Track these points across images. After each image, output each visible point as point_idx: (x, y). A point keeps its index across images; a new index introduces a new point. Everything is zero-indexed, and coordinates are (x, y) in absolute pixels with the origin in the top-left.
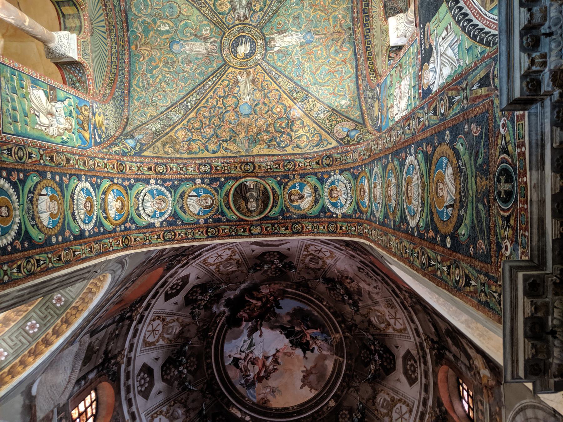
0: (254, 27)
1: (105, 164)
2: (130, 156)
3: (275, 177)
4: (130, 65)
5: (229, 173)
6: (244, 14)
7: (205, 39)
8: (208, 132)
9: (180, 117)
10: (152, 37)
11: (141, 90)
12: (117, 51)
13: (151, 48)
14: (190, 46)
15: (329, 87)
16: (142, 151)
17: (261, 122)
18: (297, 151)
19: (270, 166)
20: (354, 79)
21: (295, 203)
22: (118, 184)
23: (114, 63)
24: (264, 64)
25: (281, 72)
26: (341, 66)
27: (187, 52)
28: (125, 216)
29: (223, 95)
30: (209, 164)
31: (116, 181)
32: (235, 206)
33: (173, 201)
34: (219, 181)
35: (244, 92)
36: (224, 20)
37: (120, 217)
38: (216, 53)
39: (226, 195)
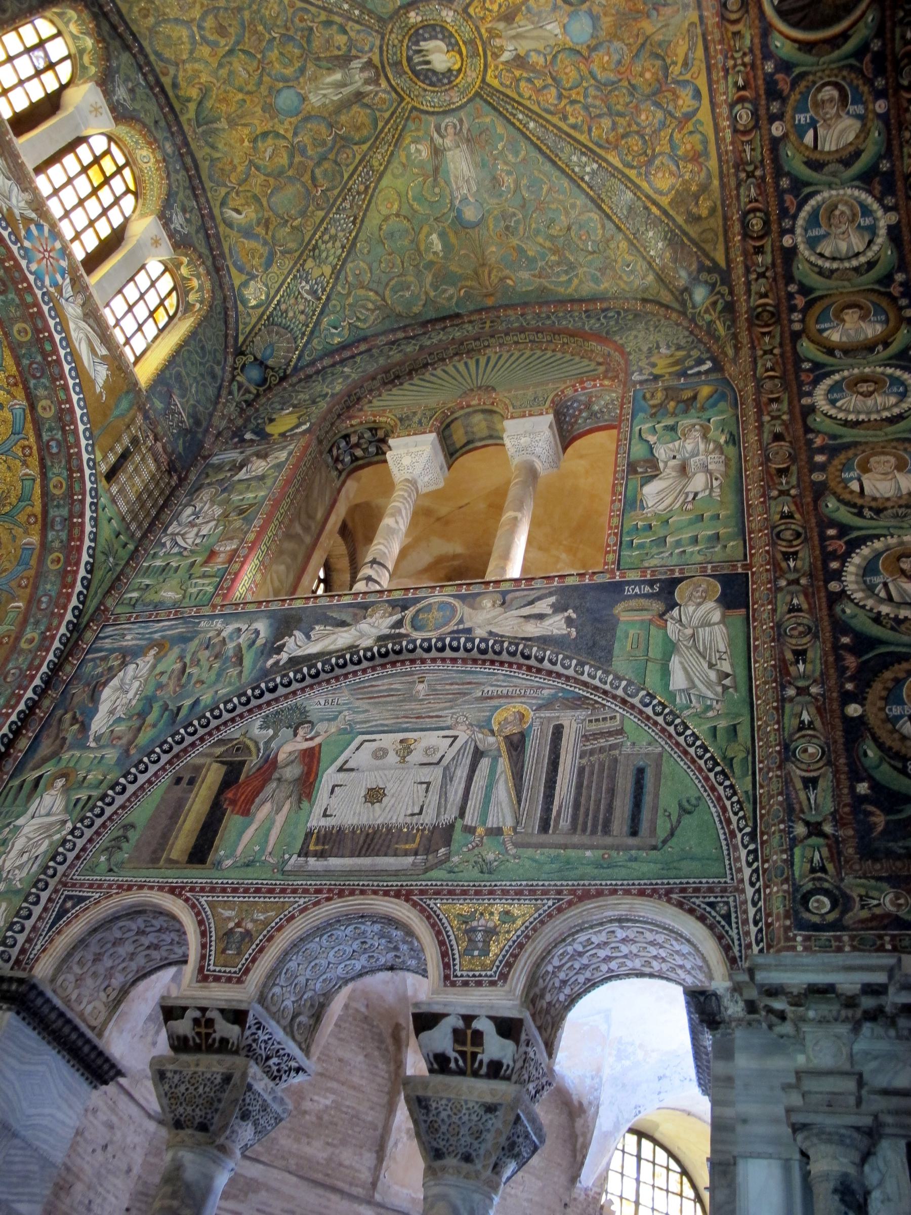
0: (383, 38)
1: (765, 352)
2: (731, 293)
4: (525, 304)
5: (751, 50)
6: (362, 70)
8: (649, 116)
9: (623, 187)
12: (507, 334)
13: (483, 265)
14: (460, 183)
16: (715, 268)
22: (803, 321)
27: (474, 189)
28: (874, 297)
29: (554, 91)
30: (732, 106)
31: (797, 327)
33: (830, 186)
34: (772, 75)
35: (538, 38)
36: (387, 115)
37: (879, 310)
38: (461, 121)
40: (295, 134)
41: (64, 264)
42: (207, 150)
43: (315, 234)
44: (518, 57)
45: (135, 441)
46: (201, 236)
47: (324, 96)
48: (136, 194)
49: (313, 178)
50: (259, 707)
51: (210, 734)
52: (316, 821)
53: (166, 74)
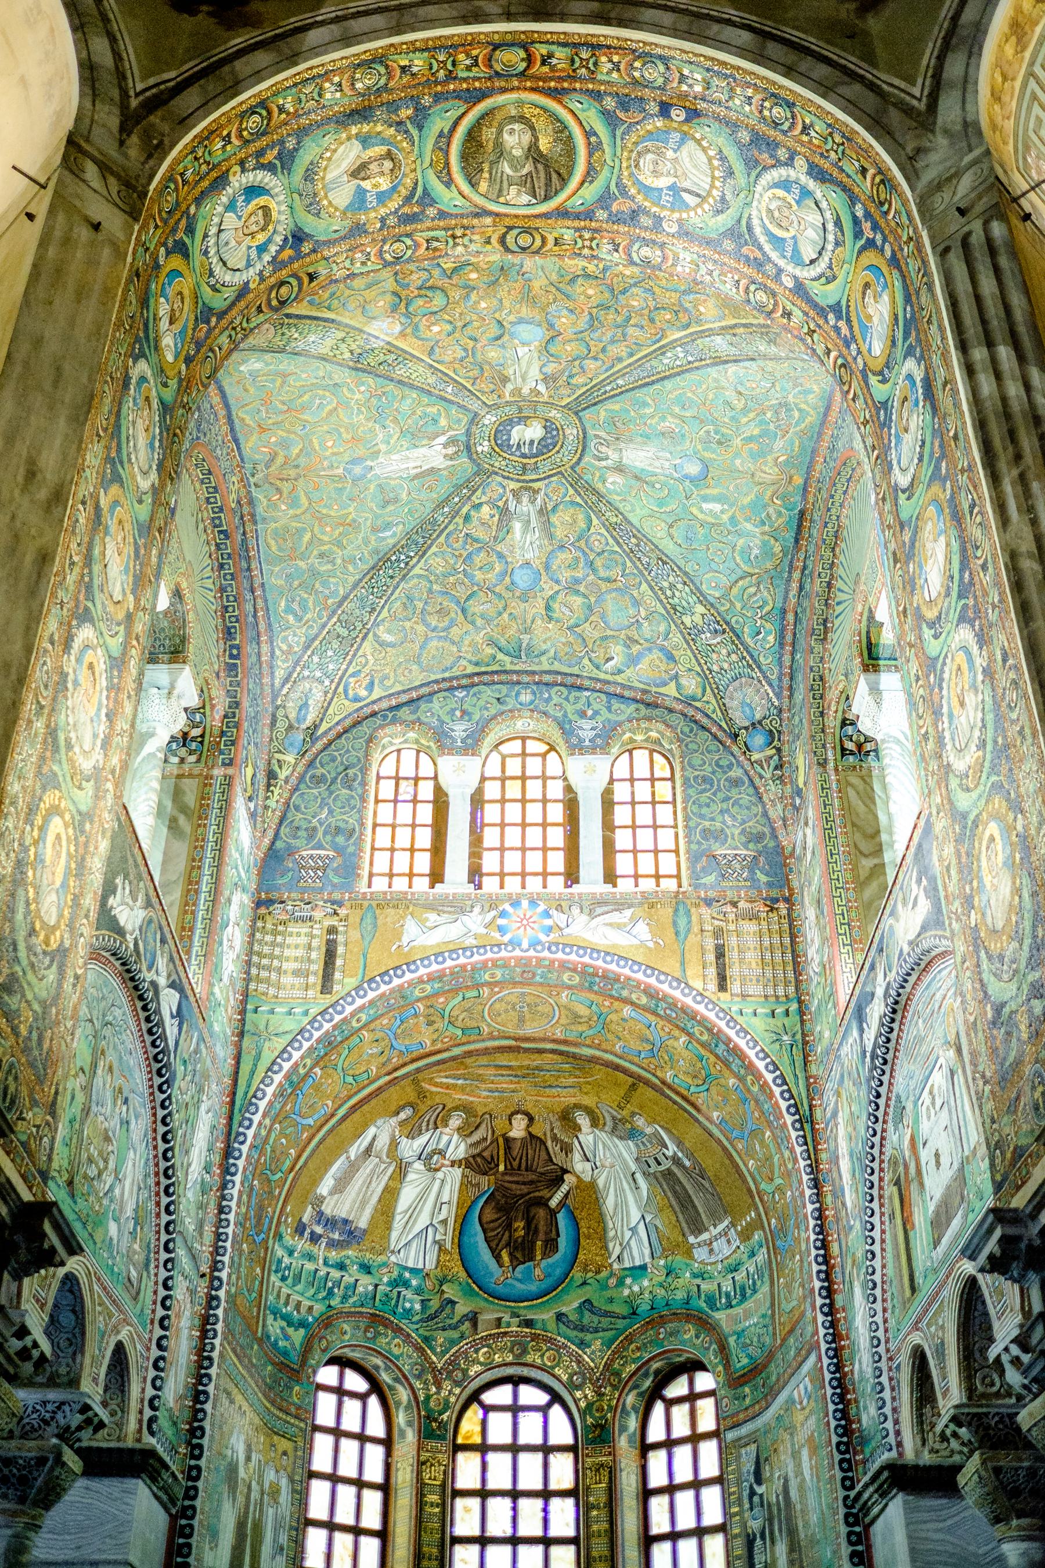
3: (442, 215)
4: (814, 452)
5: (577, 230)
7: (620, 469)
19: (455, 245)
20: (232, 402)
21: (380, 150)
22: (859, 352)
24: (475, 406)
25: (429, 393)
32: (570, 137)
33: (748, 204)
35: (529, 363)
36: (571, 491)
38: (597, 436)
39: (597, 172)
40: (557, 582)
41: (542, 907)
42: (543, 659)
44: (545, 380)
45: (718, 933)
46: (616, 705)
48: (552, 748)
49: (608, 580)
50: (886, 1113)
51: (882, 1161)
52: (932, 1207)
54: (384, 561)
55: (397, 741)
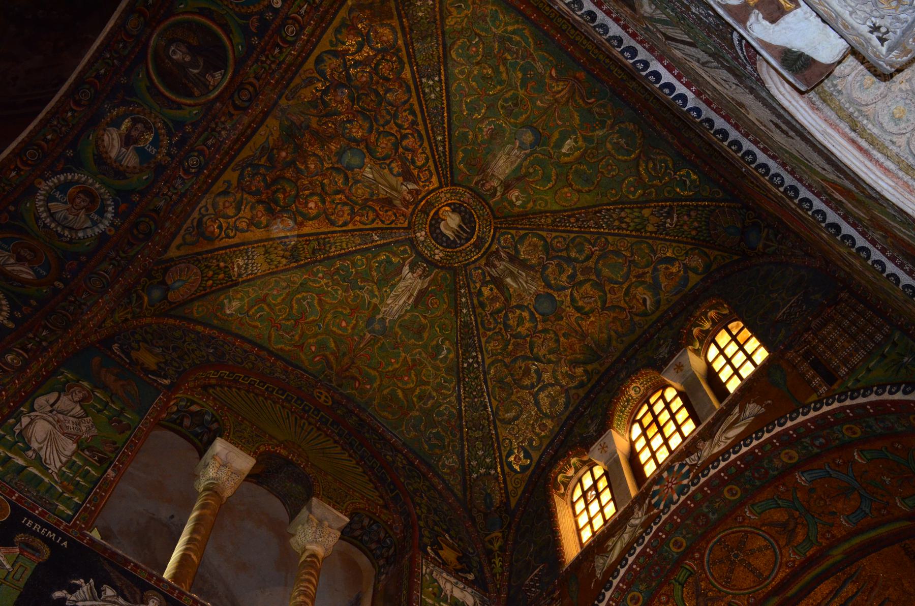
3: (194, 125)
6: (495, 267)
10: (572, 117)
11: (506, 31)
13: (556, 101)
14: (513, 158)
15: (279, 300)
17: (312, 166)
18: (219, 186)
19: (219, 133)
20: (259, 341)
23: (573, 31)
26: (297, 337)
27: (509, 146)
29: (404, 143)
30: (292, 44)
35: (382, 176)
38: (477, 183)
40: (564, 288)
42: (614, 343)
43: (627, 236)
44: (405, 180)
47: (526, 282)
49: (588, 258)
53: (579, 396)
54: (458, 372)
55: (571, 473)
